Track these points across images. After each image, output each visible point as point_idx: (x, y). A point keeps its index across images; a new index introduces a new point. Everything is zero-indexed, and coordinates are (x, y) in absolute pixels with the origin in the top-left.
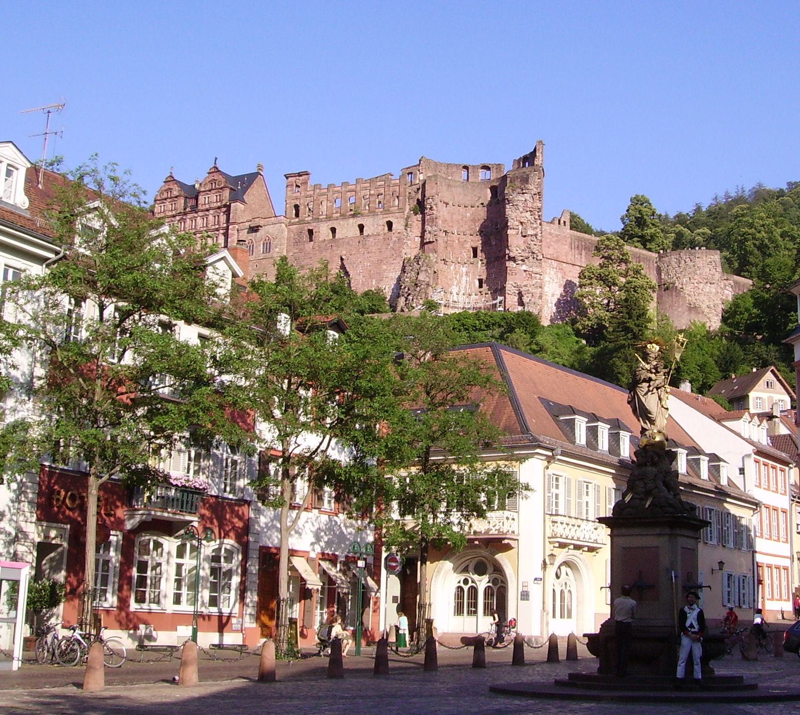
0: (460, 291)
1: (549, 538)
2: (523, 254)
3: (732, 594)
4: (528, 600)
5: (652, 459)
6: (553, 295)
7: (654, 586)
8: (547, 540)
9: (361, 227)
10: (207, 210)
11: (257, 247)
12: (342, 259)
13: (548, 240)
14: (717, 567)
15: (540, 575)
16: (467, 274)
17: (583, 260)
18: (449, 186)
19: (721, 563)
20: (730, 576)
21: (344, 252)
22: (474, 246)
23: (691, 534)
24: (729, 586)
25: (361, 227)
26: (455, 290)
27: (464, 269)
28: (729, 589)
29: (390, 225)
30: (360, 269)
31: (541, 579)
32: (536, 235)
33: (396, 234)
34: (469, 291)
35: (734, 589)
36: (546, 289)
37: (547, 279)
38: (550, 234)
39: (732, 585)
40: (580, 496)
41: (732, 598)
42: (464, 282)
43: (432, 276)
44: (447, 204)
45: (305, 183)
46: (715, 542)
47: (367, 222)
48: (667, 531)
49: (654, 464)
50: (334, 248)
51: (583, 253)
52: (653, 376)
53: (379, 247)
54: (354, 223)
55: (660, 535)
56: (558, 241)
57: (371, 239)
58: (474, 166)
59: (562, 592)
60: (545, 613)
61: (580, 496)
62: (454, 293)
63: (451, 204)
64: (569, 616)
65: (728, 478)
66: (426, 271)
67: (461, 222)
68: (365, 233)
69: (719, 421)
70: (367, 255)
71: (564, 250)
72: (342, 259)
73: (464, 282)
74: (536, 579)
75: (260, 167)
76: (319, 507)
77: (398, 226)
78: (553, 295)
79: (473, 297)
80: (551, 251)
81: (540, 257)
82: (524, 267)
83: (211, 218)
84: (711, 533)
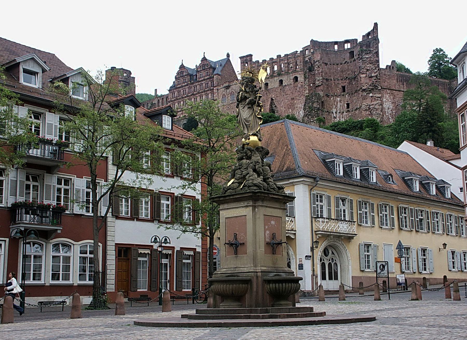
0: (337, 111)
1: (315, 232)
2: (370, 87)
3: (456, 263)
4: (302, 269)
5: (247, 155)
6: (389, 109)
7: (244, 243)
8: (314, 232)
9: (281, 82)
10: (202, 81)
11: (228, 98)
12: (272, 99)
13: (384, 78)
14: (442, 247)
15: (310, 254)
16: (340, 101)
17: (405, 87)
18: (327, 54)
19: (445, 245)
20: (453, 253)
21: (273, 96)
22: (343, 85)
23: (277, 205)
24: (453, 259)
25: (281, 82)
26: (334, 111)
27: (339, 99)
28: (453, 260)
29: (296, 79)
30: (282, 104)
31: (310, 257)
32: (376, 76)
33: (300, 83)
34: (342, 111)
35: (457, 260)
36: (384, 106)
37: (384, 100)
38: (385, 75)
39: (455, 257)
40: (338, 206)
41: (456, 265)
42: (339, 106)
43: (321, 104)
44: (326, 64)
45: (251, 60)
46: (441, 232)
47: (284, 78)
48: (251, 203)
49: (249, 158)
50: (268, 94)
51: (405, 84)
52: (247, 95)
53: (292, 91)
54: (277, 79)
55: (247, 206)
56: (389, 78)
57: (287, 88)
58: (340, 42)
59: (330, 264)
60: (314, 277)
61: (338, 206)
62: (334, 113)
63: (329, 63)
64: (336, 278)
65: (451, 192)
66: (317, 102)
67: (335, 73)
68: (284, 84)
69: (447, 161)
70: (285, 96)
71: (394, 83)
72: (272, 99)
73: (339, 106)
74: (306, 256)
75: (228, 55)
76: (159, 219)
77: (301, 79)
78: (389, 109)
79: (345, 113)
80: (386, 84)
81: (380, 88)
82: (371, 95)
83: (204, 85)
84: (451, 229)
